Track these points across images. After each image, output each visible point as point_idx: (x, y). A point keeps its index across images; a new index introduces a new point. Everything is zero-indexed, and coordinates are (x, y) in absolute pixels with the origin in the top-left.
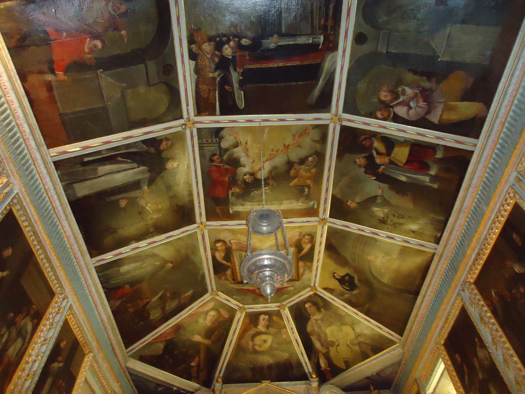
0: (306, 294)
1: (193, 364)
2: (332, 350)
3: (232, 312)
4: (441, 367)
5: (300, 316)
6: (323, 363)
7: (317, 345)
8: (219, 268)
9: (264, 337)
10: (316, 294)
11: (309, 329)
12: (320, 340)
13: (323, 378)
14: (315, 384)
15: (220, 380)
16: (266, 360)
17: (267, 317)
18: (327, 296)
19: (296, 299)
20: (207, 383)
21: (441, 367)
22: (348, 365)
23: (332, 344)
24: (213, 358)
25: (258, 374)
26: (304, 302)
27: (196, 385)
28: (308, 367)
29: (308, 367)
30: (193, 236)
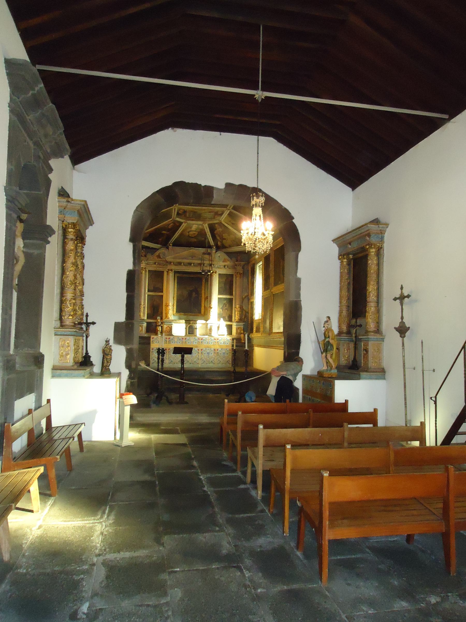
0: (215, 222)
1: (160, 240)
2: (224, 241)
3: (181, 223)
4: (261, 263)
5: (212, 228)
6: (219, 243)
7: (218, 238)
8: (178, 214)
9: (194, 232)
10: (221, 223)
11: (215, 232)
12: (219, 236)
13: (218, 248)
14: (214, 251)
15: (171, 245)
16: (194, 240)
17: (197, 226)
18: (226, 225)
19: (211, 222)
20: (165, 244)
21: (261, 263)
22: (230, 246)
23: (225, 239)
24: (169, 238)
25: (189, 245)
26: (215, 224)
27: (159, 246)
28: (212, 243)
29: (212, 243)
30: (172, 209)
